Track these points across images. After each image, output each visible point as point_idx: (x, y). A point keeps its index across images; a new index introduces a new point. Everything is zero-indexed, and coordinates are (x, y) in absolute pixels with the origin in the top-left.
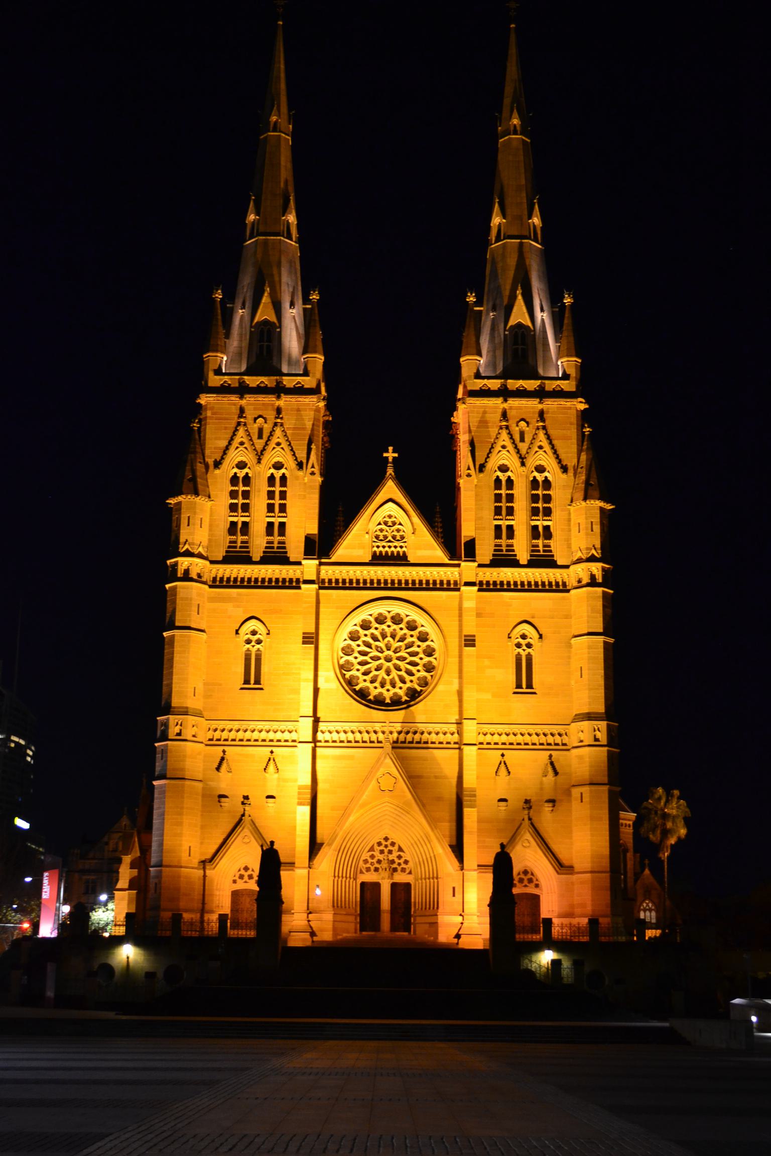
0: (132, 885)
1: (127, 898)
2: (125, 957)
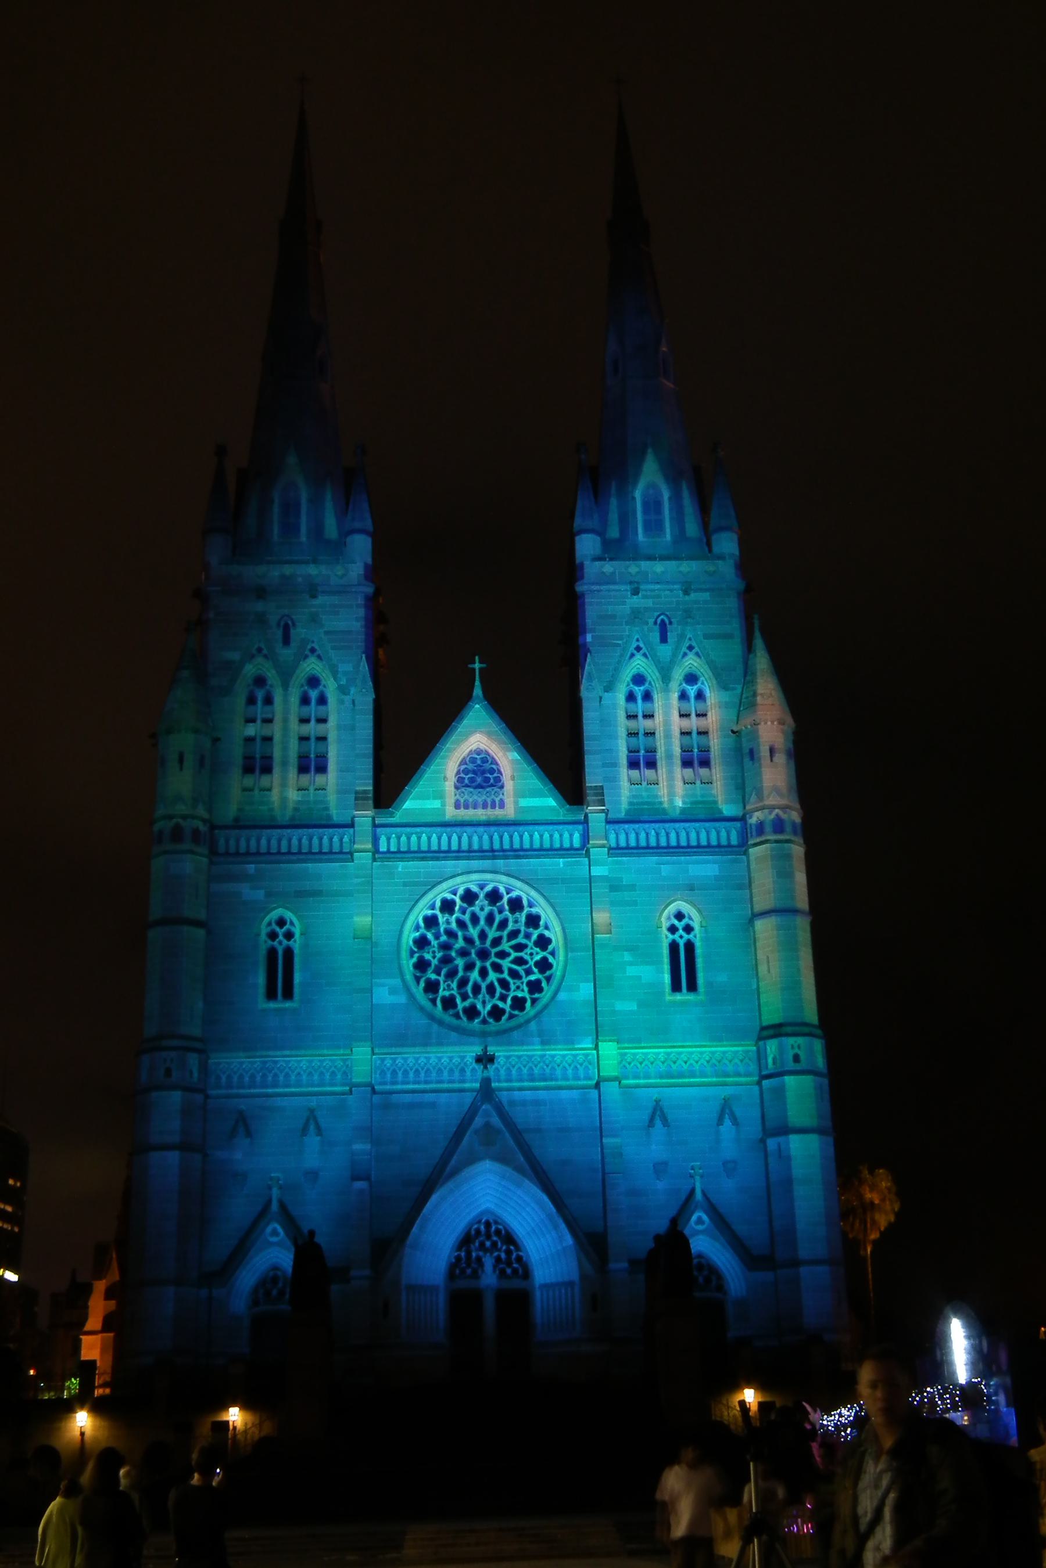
0: (108, 1324)
1: (99, 1343)
2: (77, 1433)
